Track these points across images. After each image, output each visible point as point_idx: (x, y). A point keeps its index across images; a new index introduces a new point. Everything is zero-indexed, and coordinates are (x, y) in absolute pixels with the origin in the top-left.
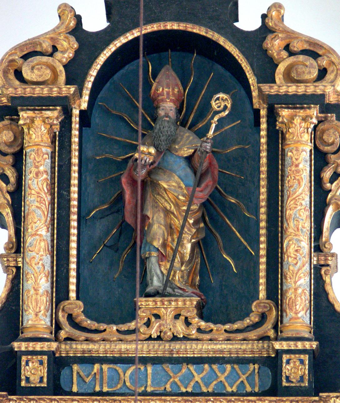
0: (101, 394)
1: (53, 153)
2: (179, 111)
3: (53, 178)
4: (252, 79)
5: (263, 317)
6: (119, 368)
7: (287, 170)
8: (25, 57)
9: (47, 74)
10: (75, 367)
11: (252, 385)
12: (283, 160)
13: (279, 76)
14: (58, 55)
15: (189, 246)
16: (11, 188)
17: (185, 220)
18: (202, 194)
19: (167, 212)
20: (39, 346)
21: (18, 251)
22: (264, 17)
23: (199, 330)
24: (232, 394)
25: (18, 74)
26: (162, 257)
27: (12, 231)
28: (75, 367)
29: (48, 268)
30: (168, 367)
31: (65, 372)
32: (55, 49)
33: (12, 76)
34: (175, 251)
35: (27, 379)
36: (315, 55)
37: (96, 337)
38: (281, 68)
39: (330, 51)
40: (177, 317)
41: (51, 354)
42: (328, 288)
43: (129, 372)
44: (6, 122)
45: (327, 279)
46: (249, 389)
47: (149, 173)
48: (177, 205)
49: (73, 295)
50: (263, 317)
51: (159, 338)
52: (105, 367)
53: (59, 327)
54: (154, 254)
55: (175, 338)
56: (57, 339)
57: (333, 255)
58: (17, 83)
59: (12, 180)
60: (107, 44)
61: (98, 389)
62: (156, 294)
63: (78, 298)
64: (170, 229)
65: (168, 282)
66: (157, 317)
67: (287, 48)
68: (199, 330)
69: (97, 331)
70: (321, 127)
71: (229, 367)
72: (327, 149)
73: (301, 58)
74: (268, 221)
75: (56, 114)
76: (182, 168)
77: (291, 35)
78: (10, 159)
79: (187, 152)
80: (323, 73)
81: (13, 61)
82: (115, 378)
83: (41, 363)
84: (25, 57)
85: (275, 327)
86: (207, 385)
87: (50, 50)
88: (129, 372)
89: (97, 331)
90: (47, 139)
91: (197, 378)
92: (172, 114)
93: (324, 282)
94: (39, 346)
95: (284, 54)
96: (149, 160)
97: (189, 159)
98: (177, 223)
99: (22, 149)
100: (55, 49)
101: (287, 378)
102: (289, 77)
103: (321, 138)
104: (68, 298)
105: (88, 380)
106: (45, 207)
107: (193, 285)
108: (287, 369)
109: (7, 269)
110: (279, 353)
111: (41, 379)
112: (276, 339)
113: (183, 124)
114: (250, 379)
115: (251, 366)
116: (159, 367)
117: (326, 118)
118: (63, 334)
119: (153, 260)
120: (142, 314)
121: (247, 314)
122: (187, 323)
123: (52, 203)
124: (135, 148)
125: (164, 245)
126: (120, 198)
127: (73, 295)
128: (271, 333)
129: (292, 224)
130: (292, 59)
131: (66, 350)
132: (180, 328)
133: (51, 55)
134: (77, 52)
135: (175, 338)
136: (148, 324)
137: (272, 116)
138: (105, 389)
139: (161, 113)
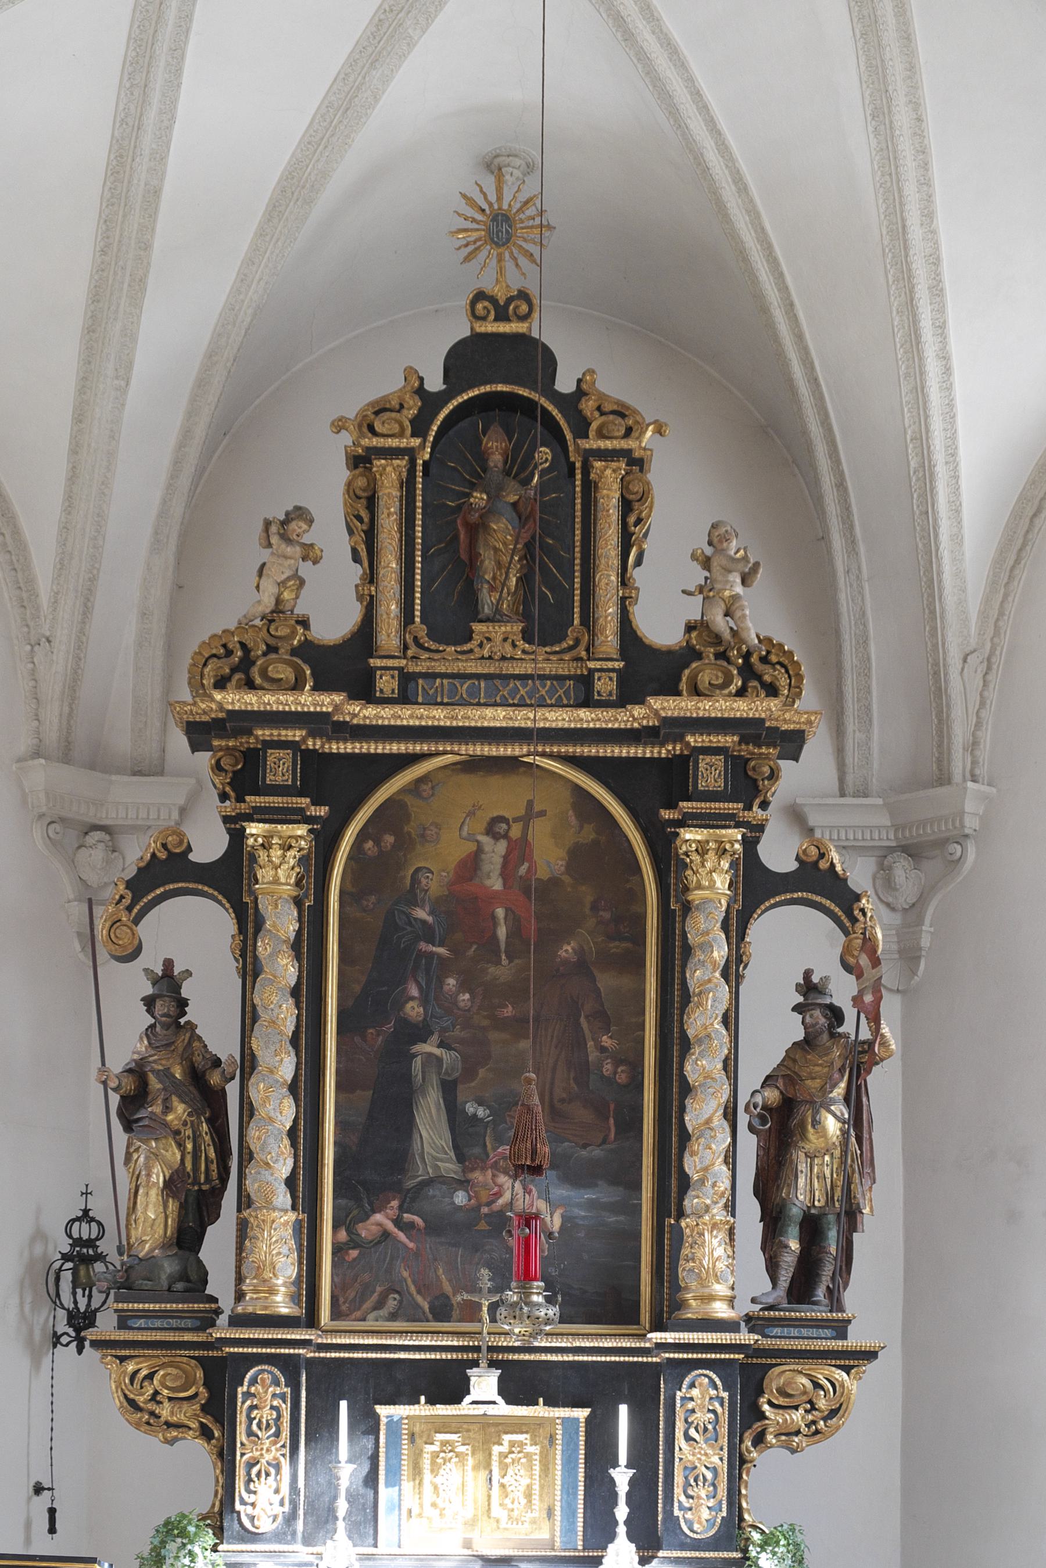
0: (442, 704)
1: (401, 496)
2: (506, 462)
3: (401, 519)
4: (569, 436)
5: (577, 642)
6: (457, 682)
7: (599, 515)
8: (377, 413)
9: (396, 428)
10: (420, 681)
11: (568, 699)
12: (595, 505)
13: (592, 433)
14: (405, 412)
15: (514, 579)
16: (365, 528)
17: (512, 558)
18: (525, 537)
19: (496, 550)
20: (390, 663)
21: (371, 582)
22: (579, 381)
23: (524, 652)
24: (552, 705)
25: (371, 429)
26: (492, 589)
27: (366, 564)
28: (420, 681)
29: (398, 596)
30: (498, 682)
31: (411, 685)
32: (402, 406)
33: (365, 430)
34: (504, 584)
35: (381, 691)
36: (623, 416)
37: (437, 656)
38: (594, 426)
39: (635, 412)
40: (505, 640)
41: (401, 670)
42: (631, 617)
43: (465, 686)
44: (361, 470)
45: (630, 609)
46: (565, 702)
47: (481, 517)
48: (505, 544)
49: (417, 620)
50: (577, 642)
51: (490, 658)
52: (445, 681)
53: (406, 647)
54: (486, 586)
55: (503, 658)
56: (405, 657)
57: (637, 589)
58: (370, 435)
59: (366, 520)
60: (446, 403)
61: (439, 700)
62: (487, 620)
63: (422, 622)
64: (499, 565)
65: (498, 610)
66: (489, 639)
67: (599, 408)
68: (524, 652)
69: (437, 651)
70: (627, 478)
71: (549, 683)
72: (631, 497)
73: (611, 417)
74: (582, 559)
75: (404, 462)
76: (509, 512)
77: (602, 396)
78: (364, 502)
79: (513, 498)
80: (629, 432)
81: (366, 416)
82: (453, 691)
83: (393, 677)
84: (377, 413)
85: (587, 650)
86: (530, 698)
87: (397, 407)
88: (465, 686)
89: (437, 651)
90: (397, 484)
91: (522, 692)
92: (500, 465)
93: (628, 612)
94: (390, 663)
95: (597, 414)
96: (483, 504)
97: (515, 505)
98: (505, 559)
99: (375, 492)
100: (402, 406)
101: (598, 692)
102: (601, 435)
103: (627, 488)
104: (413, 622)
105: (431, 692)
106: (395, 543)
107: (517, 613)
108: (598, 685)
109: (360, 598)
110: (591, 672)
111: (393, 690)
112: (589, 660)
113: (508, 473)
114: (566, 693)
115: (568, 682)
116: (490, 682)
117: (631, 470)
118: (410, 653)
119: (485, 591)
120: (477, 638)
121: (563, 638)
122: (514, 645)
123: (401, 540)
124: (469, 495)
125: (494, 578)
126: (456, 537)
127: (417, 620)
128: (584, 654)
129: (603, 561)
130: (603, 418)
131: (413, 668)
132: (508, 650)
133: (399, 411)
134: (420, 410)
135: (503, 658)
136: (481, 645)
137: (586, 469)
138: (446, 700)
139: (492, 464)
